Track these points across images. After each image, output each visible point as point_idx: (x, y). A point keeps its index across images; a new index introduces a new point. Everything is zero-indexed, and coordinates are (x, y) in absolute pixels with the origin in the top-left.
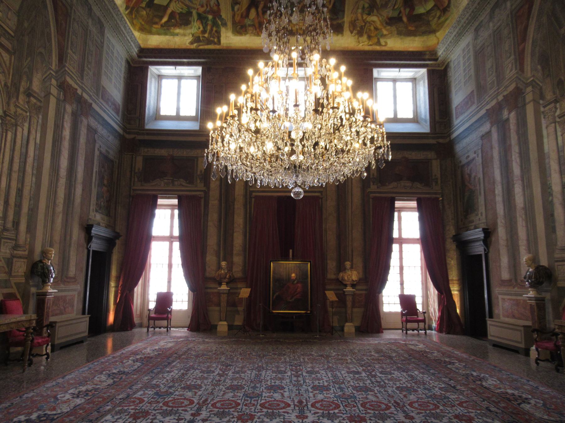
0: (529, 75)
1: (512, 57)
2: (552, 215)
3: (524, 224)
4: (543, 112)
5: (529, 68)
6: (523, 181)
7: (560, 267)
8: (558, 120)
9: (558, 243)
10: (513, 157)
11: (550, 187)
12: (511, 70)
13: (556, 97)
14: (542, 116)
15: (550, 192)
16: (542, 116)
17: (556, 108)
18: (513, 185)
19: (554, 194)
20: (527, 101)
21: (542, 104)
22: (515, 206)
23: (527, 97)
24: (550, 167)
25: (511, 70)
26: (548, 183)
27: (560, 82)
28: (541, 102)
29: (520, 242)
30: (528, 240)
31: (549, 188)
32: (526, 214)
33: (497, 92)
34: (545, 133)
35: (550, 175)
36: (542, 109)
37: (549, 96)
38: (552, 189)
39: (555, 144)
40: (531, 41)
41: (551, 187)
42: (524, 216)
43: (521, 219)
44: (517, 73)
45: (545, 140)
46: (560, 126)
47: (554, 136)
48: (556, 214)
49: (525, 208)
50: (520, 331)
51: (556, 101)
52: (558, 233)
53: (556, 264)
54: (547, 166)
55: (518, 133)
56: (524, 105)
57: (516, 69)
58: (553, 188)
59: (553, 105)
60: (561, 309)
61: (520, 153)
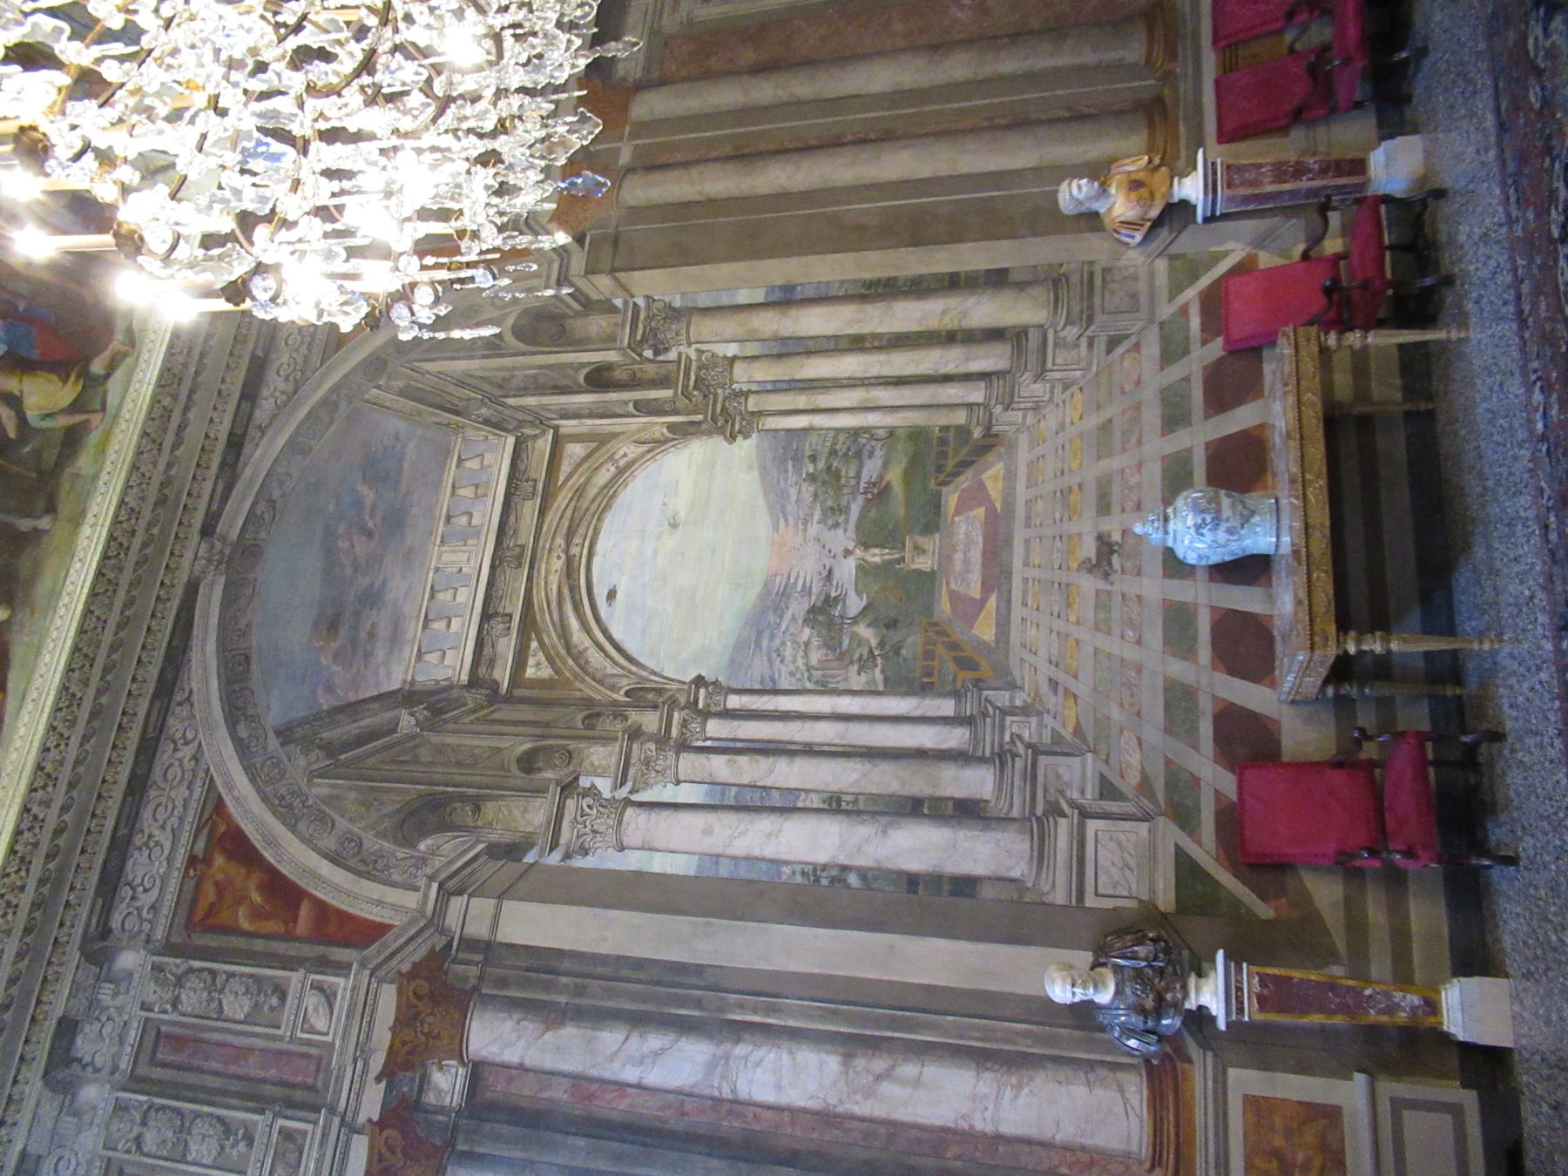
0: (411, 900)
1: (295, 979)
2: (912, 881)
3: (909, 1069)
4: (567, 856)
5: (393, 895)
6: (739, 1030)
7: (1102, 878)
8: (623, 793)
9: (1016, 874)
10: (631, 1075)
11: (815, 872)
12: (329, 996)
13: (558, 783)
14: (579, 862)
15: (833, 880)
16: (579, 862)
17: (592, 792)
18: (736, 1106)
19: (843, 859)
20: (478, 929)
21: (541, 854)
22: (826, 1118)
23: (470, 930)
24: (750, 859)
25: (329, 996)
26: (799, 879)
27: (528, 763)
28: (530, 858)
29: (979, 1125)
30: (982, 1058)
31: (817, 880)
32: (875, 1045)
33: (337, 1121)
34: (632, 861)
35: (777, 863)
36: (554, 859)
37: (533, 815)
38: (825, 867)
39: (686, 817)
40: (326, 868)
41: (815, 866)
42: (880, 1065)
43: (886, 1088)
44: (363, 965)
45: (659, 864)
46: (647, 785)
47: (665, 813)
48: (914, 866)
49: (851, 1045)
50: (1398, 1105)
51: (568, 787)
52: (979, 870)
53: (1090, 901)
54: (743, 873)
55: (552, 1015)
56: (488, 949)
57: (342, 968)
58: (822, 857)
59: (571, 804)
60: (1264, 911)
61: (639, 1021)
